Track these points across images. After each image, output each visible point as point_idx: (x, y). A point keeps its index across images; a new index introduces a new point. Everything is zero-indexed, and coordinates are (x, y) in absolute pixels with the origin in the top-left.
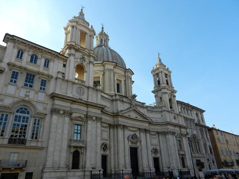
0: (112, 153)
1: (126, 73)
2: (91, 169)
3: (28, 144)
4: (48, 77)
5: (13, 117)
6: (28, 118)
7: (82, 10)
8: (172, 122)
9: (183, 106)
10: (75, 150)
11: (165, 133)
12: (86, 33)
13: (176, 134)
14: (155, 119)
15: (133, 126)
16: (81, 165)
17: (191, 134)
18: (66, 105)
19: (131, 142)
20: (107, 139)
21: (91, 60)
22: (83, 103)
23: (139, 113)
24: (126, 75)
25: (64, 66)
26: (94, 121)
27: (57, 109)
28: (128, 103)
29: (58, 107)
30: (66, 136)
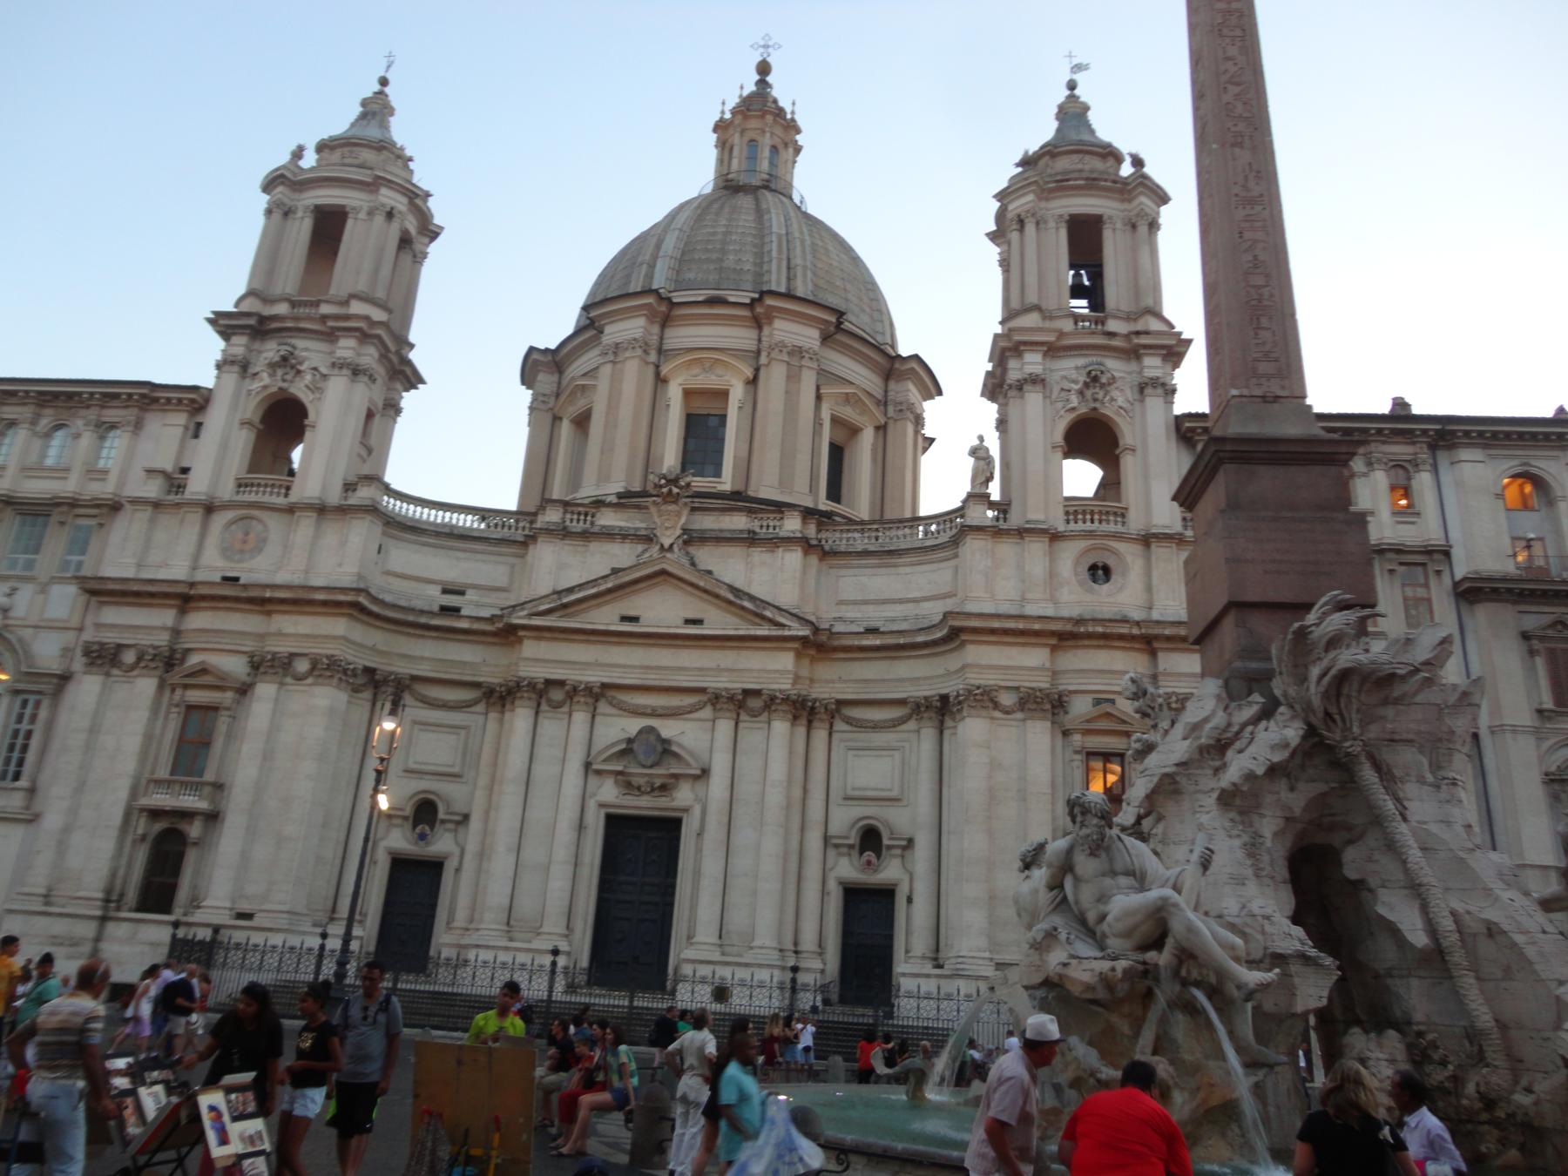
0: (472, 847)
1: (766, 331)
2: (224, 918)
4: (98, 506)
7: (384, 82)
8: (1031, 610)
10: (159, 826)
11: (942, 709)
13: (1080, 707)
14: (910, 605)
15: (652, 679)
16: (182, 895)
19: (616, 782)
20: (456, 770)
21: (340, 353)
22: (237, 599)
23: (706, 591)
24: (765, 344)
26: (299, 678)
27: (102, 644)
28: (624, 536)
29: (110, 637)
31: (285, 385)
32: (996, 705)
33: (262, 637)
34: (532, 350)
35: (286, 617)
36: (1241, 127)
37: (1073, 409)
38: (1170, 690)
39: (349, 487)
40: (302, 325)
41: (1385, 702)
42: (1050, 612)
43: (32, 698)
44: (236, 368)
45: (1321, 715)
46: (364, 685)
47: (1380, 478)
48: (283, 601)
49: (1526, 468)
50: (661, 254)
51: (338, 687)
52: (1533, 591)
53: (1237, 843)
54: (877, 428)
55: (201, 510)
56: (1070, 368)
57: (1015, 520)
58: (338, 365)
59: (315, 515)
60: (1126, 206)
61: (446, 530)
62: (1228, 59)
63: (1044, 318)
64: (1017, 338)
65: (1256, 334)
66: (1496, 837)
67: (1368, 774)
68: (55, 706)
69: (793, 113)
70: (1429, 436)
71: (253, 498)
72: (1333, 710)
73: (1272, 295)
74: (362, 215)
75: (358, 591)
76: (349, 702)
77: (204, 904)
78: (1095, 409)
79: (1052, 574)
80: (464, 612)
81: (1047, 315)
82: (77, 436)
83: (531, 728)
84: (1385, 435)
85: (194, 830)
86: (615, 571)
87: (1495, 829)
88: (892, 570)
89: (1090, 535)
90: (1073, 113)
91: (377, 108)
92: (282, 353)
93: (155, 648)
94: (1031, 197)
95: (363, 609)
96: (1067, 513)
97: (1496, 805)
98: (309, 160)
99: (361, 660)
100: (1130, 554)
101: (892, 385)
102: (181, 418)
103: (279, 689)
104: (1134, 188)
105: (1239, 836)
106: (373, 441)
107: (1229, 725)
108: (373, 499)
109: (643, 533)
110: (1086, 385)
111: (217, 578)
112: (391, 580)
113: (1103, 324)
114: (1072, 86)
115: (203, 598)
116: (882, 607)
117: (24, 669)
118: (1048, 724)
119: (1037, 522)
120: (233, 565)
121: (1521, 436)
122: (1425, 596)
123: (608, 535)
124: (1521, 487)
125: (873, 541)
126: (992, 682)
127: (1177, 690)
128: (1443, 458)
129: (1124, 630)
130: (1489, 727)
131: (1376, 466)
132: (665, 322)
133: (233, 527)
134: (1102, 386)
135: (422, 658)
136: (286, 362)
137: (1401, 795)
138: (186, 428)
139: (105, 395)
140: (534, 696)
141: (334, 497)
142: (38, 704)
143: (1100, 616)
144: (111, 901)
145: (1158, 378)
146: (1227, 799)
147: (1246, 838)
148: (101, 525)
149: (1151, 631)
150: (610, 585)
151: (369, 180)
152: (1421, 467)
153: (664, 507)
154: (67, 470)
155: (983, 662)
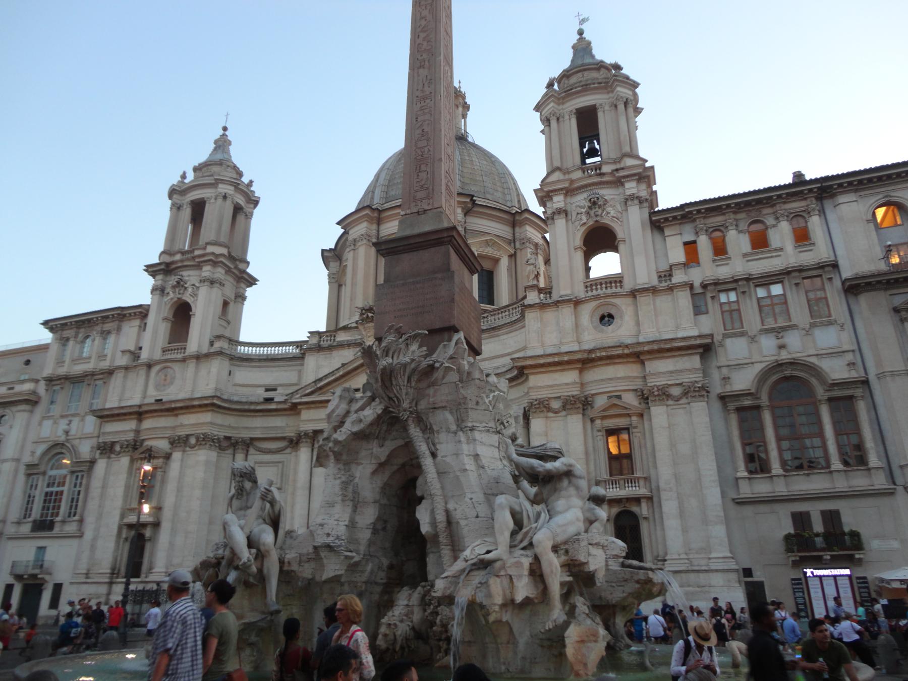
3: (57, 529)
4: (102, 373)
5: (44, 480)
6: (65, 477)
7: (225, 129)
8: (564, 349)
9: (717, 220)
12: (203, 198)
13: (601, 402)
17: (758, 368)
18: (123, 429)
21: (204, 274)
22: (161, 411)
25: (143, 327)
26: (192, 447)
27: (105, 443)
29: (109, 439)
30: (119, 503)
31: (180, 296)
32: (549, 409)
33: (174, 428)
34: (323, 251)
35: (184, 416)
36: (425, 56)
37: (585, 224)
38: (653, 384)
39: (212, 344)
40: (186, 263)
41: (429, 386)
42: (576, 348)
43: (80, 474)
44: (158, 292)
45: (386, 399)
46: (228, 446)
47: (785, 227)
48: (181, 408)
49: (887, 199)
50: (378, 184)
51: (210, 449)
52: (896, 280)
53: (338, 482)
54: (510, 256)
55: (145, 368)
56: (581, 200)
57: (555, 297)
58: (202, 281)
59: (195, 361)
60: (611, 95)
61: (265, 357)
62: (423, 18)
63: (564, 174)
64: (546, 189)
65: (418, 175)
66: (888, 448)
67: (415, 432)
68: (89, 477)
69: (460, 87)
70: (815, 192)
71: (169, 357)
72: (392, 395)
73: (429, 150)
74: (213, 201)
75: (213, 397)
76: (218, 456)
77: (154, 571)
78: (597, 221)
79: (577, 325)
80: (276, 400)
81: (567, 172)
82: (93, 340)
83: (310, 457)
84: (783, 198)
85: (148, 533)
86: (343, 365)
87: (887, 443)
88: (497, 339)
89: (597, 297)
90: (582, 48)
91: (222, 144)
92: (176, 280)
93: (127, 441)
94: (552, 104)
95: (219, 407)
96: (586, 287)
97: (886, 426)
98: (190, 177)
99: (222, 434)
100: (624, 306)
101: (517, 229)
102: (137, 322)
103: (183, 454)
104: (613, 83)
105: (340, 478)
106: (230, 317)
107: (348, 413)
108: (222, 348)
109: (359, 341)
110: (590, 208)
111: (153, 401)
112: (238, 388)
113: (600, 169)
114: (581, 33)
115: (147, 412)
116: (492, 361)
117: (74, 460)
118: (580, 416)
119: (566, 295)
120: (159, 393)
121: (880, 179)
122: (823, 296)
123: (342, 346)
124: (893, 211)
125: (486, 323)
126: (545, 396)
127: (658, 384)
128: (828, 204)
129: (619, 352)
130: (876, 375)
131: (781, 219)
132: (379, 221)
133: (160, 374)
134: (600, 207)
135: (256, 428)
136: (180, 284)
137: (436, 441)
138: (140, 327)
139: (102, 317)
140: (309, 440)
141: (205, 349)
142: (82, 476)
143: (606, 346)
144: (114, 573)
145: (634, 194)
146: (338, 457)
147: (344, 479)
148: (105, 383)
149: (636, 350)
150: (341, 373)
151: (213, 182)
152: (812, 214)
153: (366, 326)
154: (90, 358)
155: (539, 385)
